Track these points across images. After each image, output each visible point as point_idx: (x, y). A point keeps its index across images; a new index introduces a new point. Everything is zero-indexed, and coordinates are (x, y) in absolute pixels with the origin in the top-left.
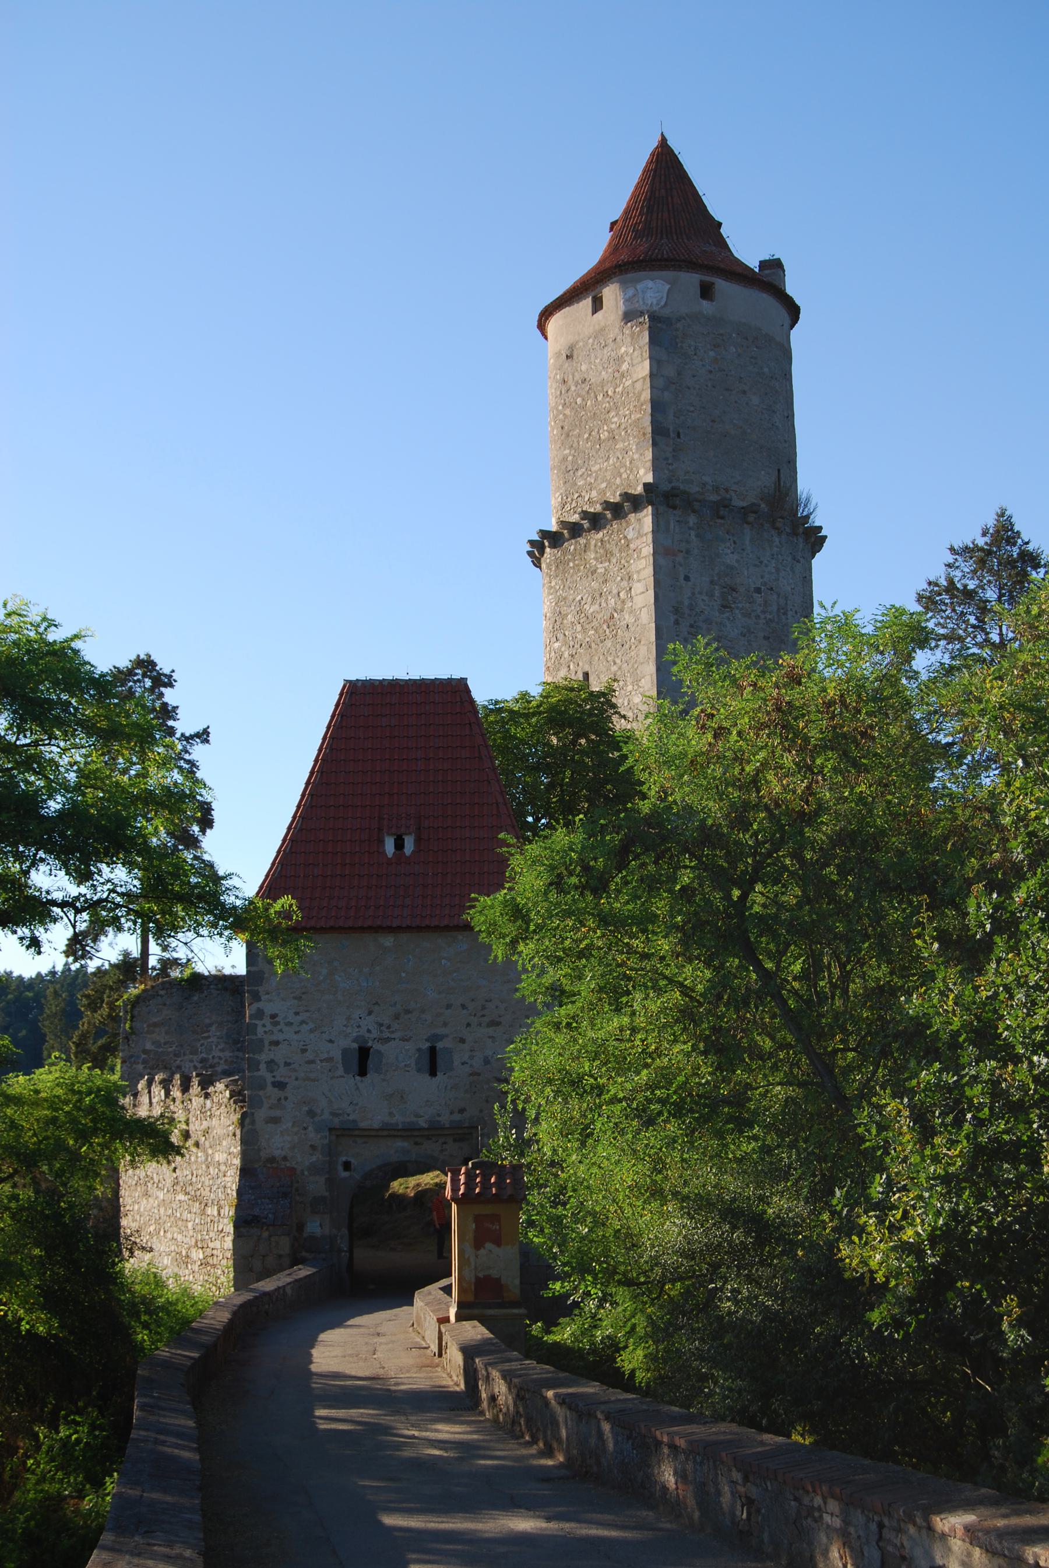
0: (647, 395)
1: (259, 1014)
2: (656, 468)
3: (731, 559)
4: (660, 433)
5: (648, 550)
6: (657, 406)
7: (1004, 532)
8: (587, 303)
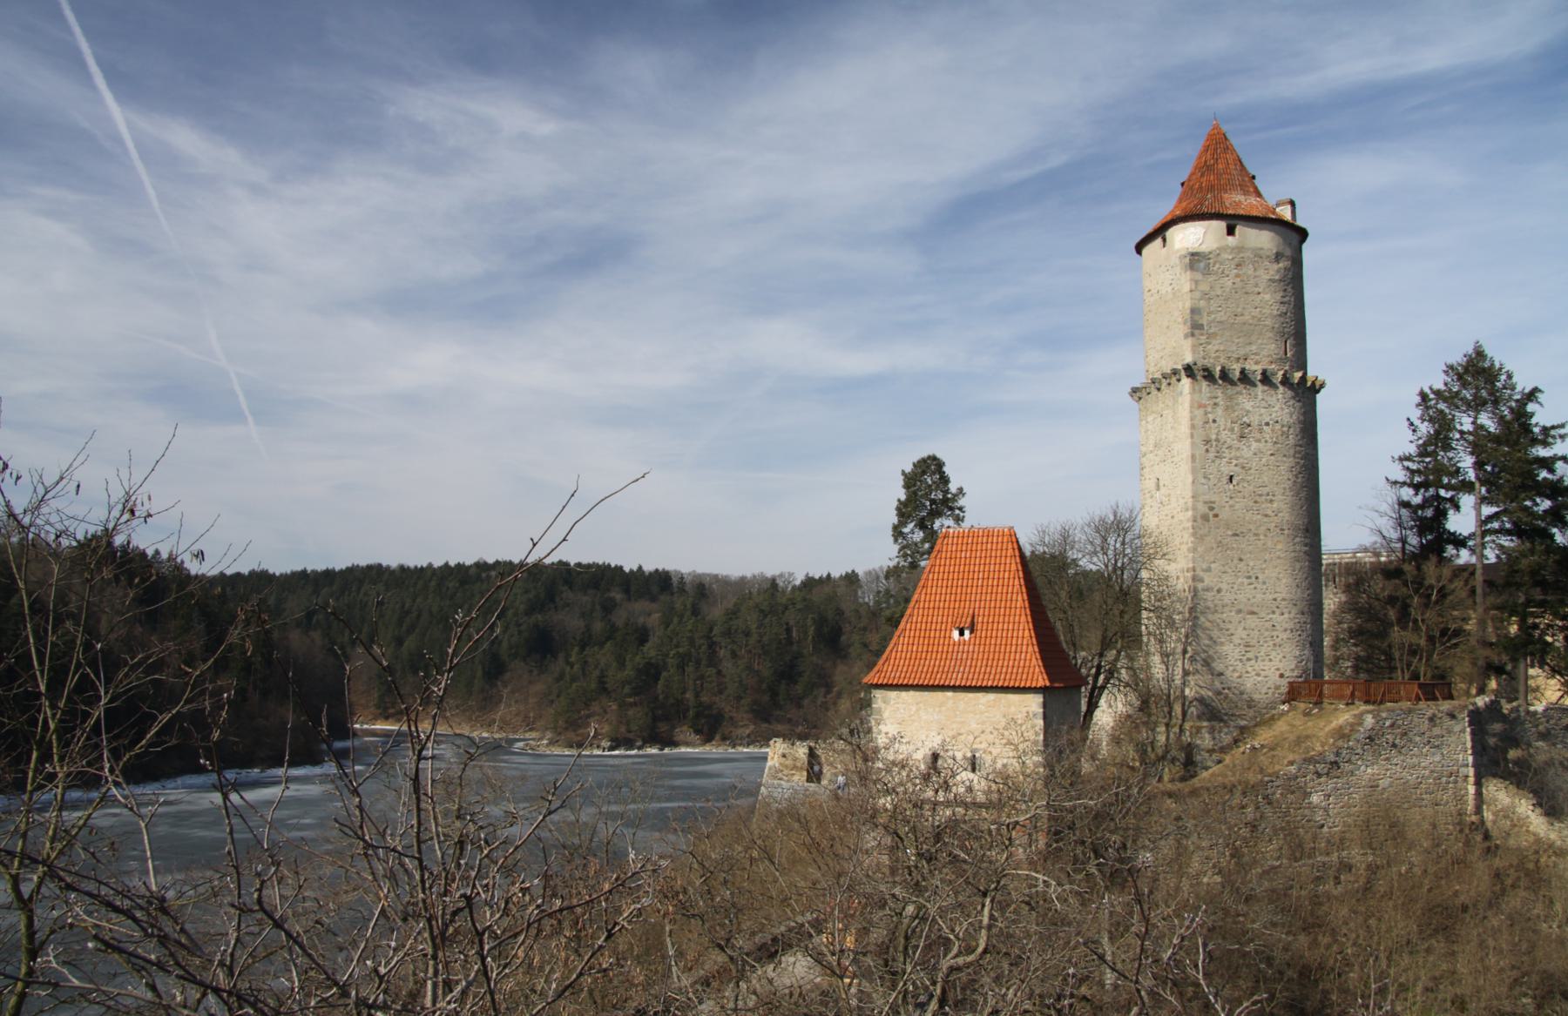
0: (1188, 305)
1: (880, 732)
2: (1194, 352)
3: (1248, 405)
4: (1195, 327)
5: (1187, 405)
6: (1194, 311)
7: (1480, 354)
8: (1159, 241)
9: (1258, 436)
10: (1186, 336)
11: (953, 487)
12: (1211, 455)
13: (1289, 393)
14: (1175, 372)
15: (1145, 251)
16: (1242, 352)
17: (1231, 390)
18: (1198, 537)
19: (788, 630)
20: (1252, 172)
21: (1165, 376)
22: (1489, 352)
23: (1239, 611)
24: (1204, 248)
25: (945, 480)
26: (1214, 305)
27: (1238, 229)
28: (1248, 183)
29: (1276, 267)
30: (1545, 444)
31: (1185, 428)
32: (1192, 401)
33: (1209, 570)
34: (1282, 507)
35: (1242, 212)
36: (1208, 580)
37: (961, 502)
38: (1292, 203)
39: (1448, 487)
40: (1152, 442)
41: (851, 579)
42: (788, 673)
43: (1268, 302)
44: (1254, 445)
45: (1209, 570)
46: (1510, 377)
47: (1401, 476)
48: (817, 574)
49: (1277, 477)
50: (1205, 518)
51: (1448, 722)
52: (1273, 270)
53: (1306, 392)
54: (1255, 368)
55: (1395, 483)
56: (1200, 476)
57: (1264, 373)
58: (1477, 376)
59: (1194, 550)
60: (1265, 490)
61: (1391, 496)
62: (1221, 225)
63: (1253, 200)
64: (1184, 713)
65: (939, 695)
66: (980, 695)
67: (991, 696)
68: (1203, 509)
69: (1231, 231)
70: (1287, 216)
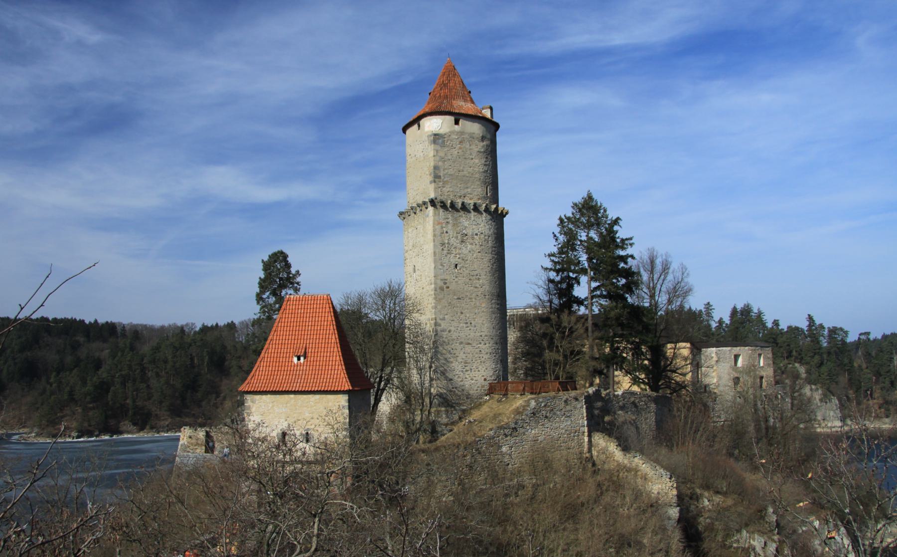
0: (432, 164)
1: (250, 420)
3: (466, 224)
4: (436, 177)
5: (431, 223)
6: (436, 168)
7: (590, 197)
8: (416, 126)
9: (471, 241)
10: (431, 182)
11: (293, 270)
12: (445, 252)
13: (489, 217)
14: (424, 203)
15: (408, 132)
16: (463, 192)
17: (456, 214)
18: (438, 299)
19: (192, 359)
20: (469, 89)
21: (419, 206)
22: (595, 197)
23: (461, 343)
24: (442, 132)
25: (288, 266)
26: (447, 164)
27: (461, 122)
28: (467, 95)
29: (482, 144)
30: (623, 248)
31: (430, 236)
32: (434, 220)
33: (444, 319)
34: (485, 282)
35: (463, 112)
36: (444, 325)
37: (298, 279)
38: (491, 108)
39: (574, 272)
40: (411, 244)
41: (231, 326)
42: (192, 385)
43: (477, 164)
44: (469, 246)
45: (444, 319)
46: (605, 211)
47: (549, 265)
48: (210, 323)
49: (482, 265)
50: (442, 289)
51: (574, 403)
52: (480, 146)
53: (498, 217)
54: (470, 202)
55: (546, 269)
56: (439, 264)
57: (475, 205)
58: (589, 209)
59: (435, 307)
60: (475, 273)
61: (544, 276)
62: (451, 119)
63: (470, 105)
64: (431, 403)
65: (286, 396)
66: (310, 396)
67: (317, 396)
68: (440, 283)
69: (457, 122)
70: (488, 115)
